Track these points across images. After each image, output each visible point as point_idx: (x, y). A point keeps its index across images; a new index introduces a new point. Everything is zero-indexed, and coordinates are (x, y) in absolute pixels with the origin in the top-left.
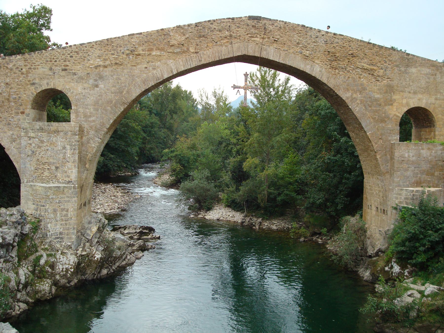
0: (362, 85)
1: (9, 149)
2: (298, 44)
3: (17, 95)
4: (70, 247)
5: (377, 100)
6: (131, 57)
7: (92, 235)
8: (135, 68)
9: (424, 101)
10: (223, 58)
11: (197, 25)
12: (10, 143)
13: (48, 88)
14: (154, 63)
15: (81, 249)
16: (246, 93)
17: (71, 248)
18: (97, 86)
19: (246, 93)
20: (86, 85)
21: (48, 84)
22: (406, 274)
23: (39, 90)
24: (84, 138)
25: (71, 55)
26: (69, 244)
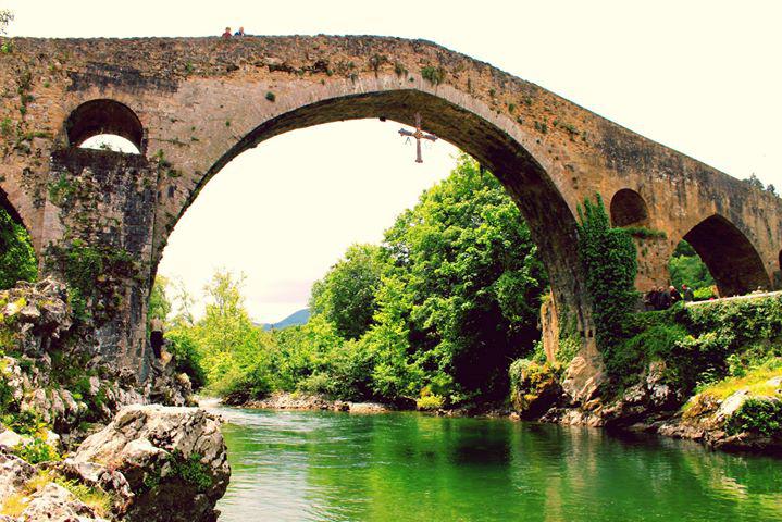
0: (564, 152)
1: (15, 195)
2: (483, 86)
3: (41, 103)
4: (132, 379)
5: (581, 173)
6: (247, 67)
7: (164, 365)
8: (251, 85)
9: (635, 183)
10: (385, 89)
11: (347, 37)
12: (19, 185)
13: (103, 97)
14: (283, 84)
15: (150, 385)
16: (419, 143)
17: (133, 380)
18: (190, 105)
19: (419, 143)
20: (171, 101)
21: (102, 91)
22: (679, 395)
23: (88, 98)
24: (162, 187)
25: (147, 50)
26: (133, 372)
